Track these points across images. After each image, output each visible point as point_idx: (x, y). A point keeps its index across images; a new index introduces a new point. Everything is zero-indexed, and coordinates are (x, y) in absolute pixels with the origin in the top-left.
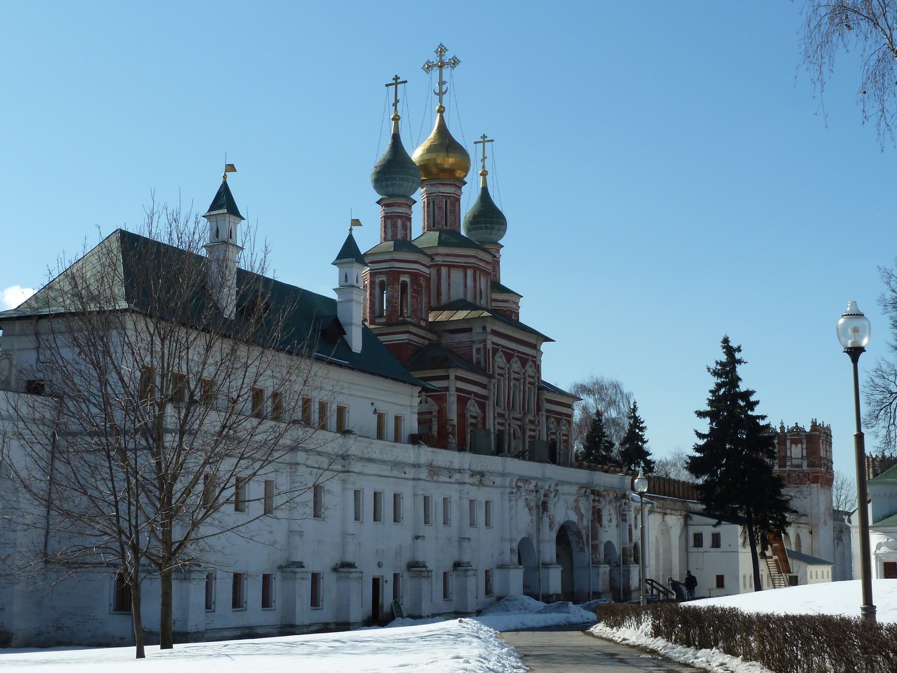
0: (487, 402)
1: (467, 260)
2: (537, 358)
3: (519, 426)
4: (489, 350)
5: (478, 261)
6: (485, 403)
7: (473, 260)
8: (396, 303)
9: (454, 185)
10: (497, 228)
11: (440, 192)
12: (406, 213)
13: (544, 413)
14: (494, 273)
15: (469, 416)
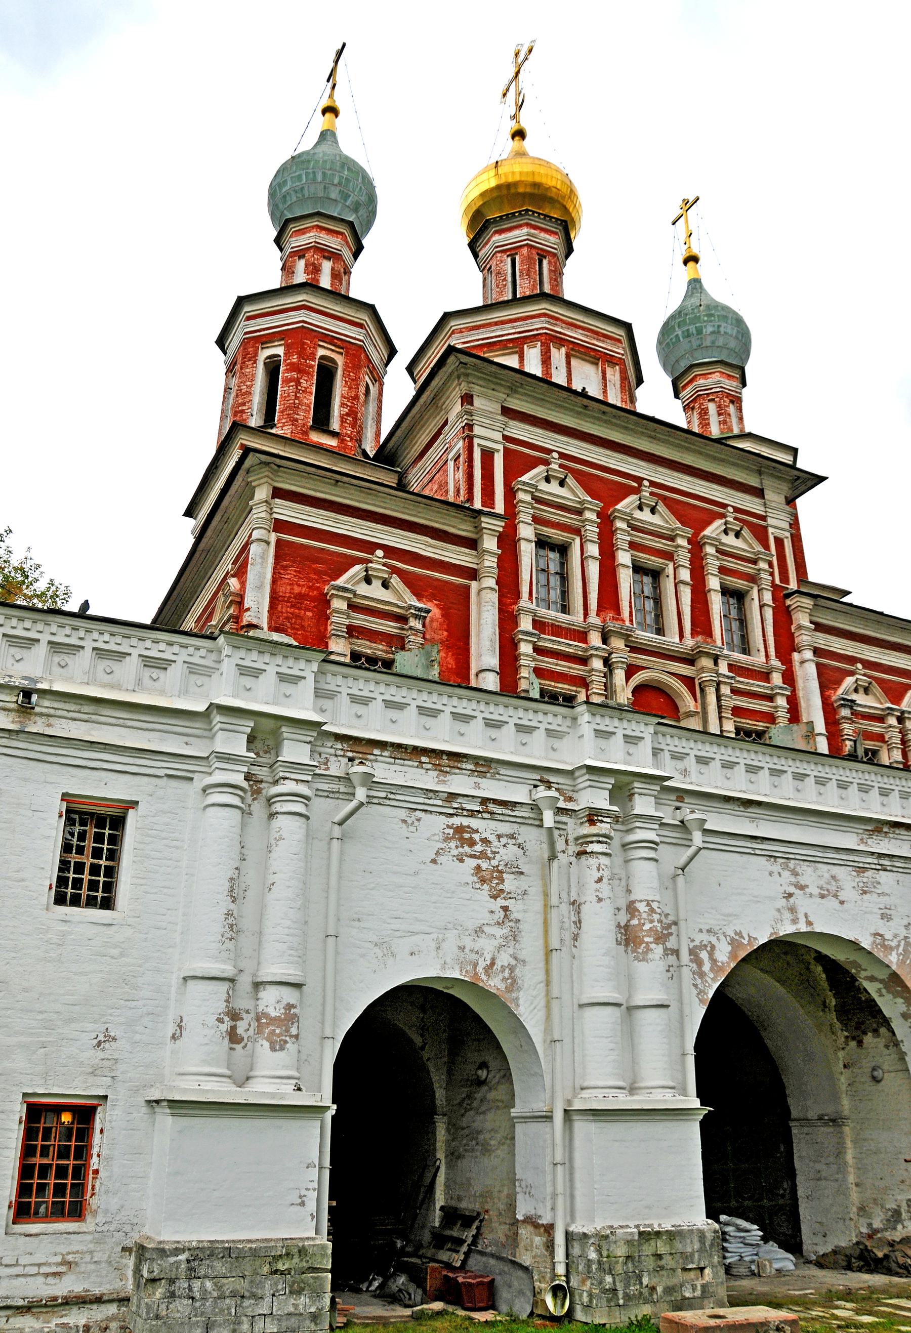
0: (474, 585)
1: (522, 326)
2: (770, 521)
3: (688, 681)
4: (488, 456)
5: (551, 324)
6: (468, 588)
7: (538, 324)
8: (244, 404)
9: (527, 225)
10: (710, 329)
11: (497, 247)
12: (315, 242)
13: (808, 654)
14: (722, 418)
15: (343, 605)
